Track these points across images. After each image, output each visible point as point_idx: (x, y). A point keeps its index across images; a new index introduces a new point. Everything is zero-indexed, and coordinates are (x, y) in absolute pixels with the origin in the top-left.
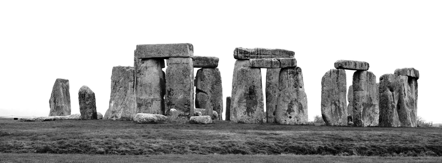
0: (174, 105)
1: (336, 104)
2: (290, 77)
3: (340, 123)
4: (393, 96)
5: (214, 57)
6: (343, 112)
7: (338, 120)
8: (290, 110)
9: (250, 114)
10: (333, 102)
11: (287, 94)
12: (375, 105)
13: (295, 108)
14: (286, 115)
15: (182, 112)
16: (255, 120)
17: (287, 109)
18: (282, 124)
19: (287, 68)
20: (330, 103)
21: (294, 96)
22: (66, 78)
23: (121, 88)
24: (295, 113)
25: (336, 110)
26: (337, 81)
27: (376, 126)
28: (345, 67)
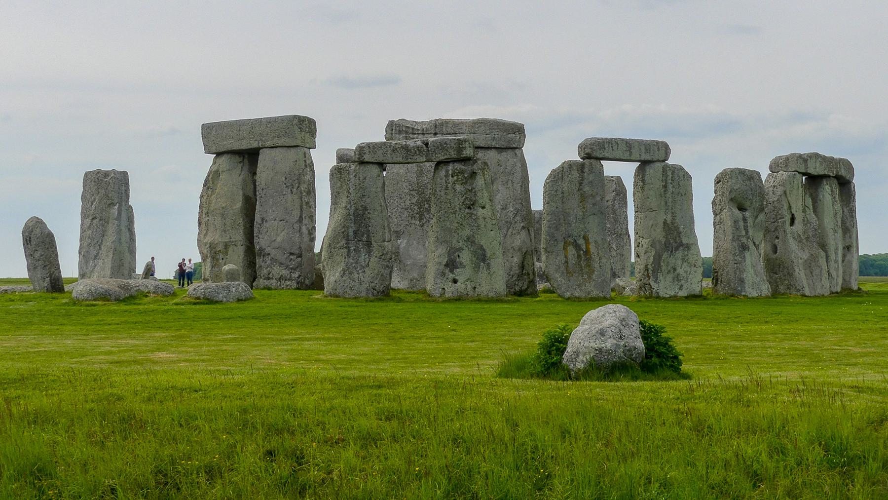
0: (269, 254)
1: (577, 247)
6: (596, 265)
12: (688, 247)
13: (466, 257)
14: (443, 274)
15: (284, 272)
19: (446, 162)
23: (95, 221)
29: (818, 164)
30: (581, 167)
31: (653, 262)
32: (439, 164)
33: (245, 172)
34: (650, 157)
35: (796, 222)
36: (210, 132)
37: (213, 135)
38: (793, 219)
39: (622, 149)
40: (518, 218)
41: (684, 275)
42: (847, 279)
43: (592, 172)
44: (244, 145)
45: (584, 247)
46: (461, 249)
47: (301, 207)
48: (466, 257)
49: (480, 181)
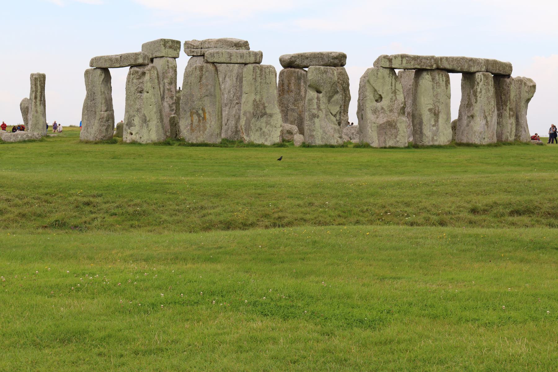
1: (199, 115)
2: (133, 79)
5: (331, 53)
6: (208, 126)
9: (89, 130)
12: (271, 116)
13: (137, 121)
20: (189, 114)
26: (200, 82)
28: (210, 60)
29: (404, 61)
31: (245, 124)
35: (383, 100)
38: (380, 99)
40: (235, 98)
41: (268, 132)
42: (469, 137)
43: (207, 71)
45: (202, 115)
46: (134, 116)
47: (164, 91)
48: (137, 121)
49: (147, 77)
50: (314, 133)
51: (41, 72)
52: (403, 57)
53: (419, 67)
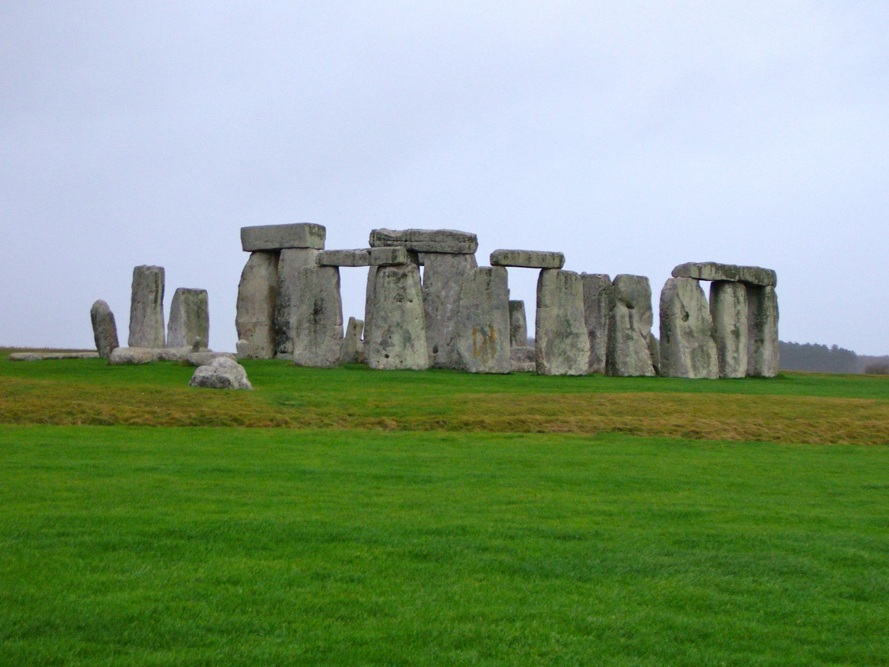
1: (484, 333)
2: (388, 283)
3: (491, 368)
4: (631, 317)
6: (498, 348)
7: (485, 362)
8: (385, 344)
9: (314, 350)
10: (479, 327)
11: (382, 313)
12: (577, 335)
13: (396, 339)
16: (322, 361)
17: (379, 340)
18: (374, 370)
20: (471, 331)
21: (396, 317)
22: (200, 287)
24: (395, 349)
25: (484, 343)
27: (580, 376)
28: (503, 262)
29: (714, 271)
30: (489, 272)
32: (381, 267)
33: (272, 268)
34: (548, 265)
35: (690, 318)
36: (246, 234)
37: (249, 238)
38: (687, 316)
39: (525, 259)
44: (270, 246)
49: (410, 281)
50: (628, 359)
51: (158, 265)
52: (713, 264)
53: (724, 278)
